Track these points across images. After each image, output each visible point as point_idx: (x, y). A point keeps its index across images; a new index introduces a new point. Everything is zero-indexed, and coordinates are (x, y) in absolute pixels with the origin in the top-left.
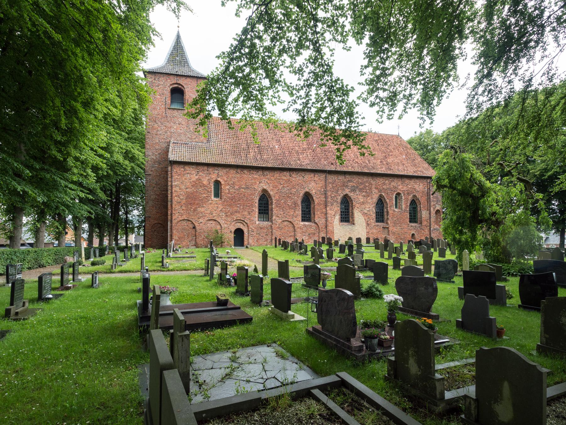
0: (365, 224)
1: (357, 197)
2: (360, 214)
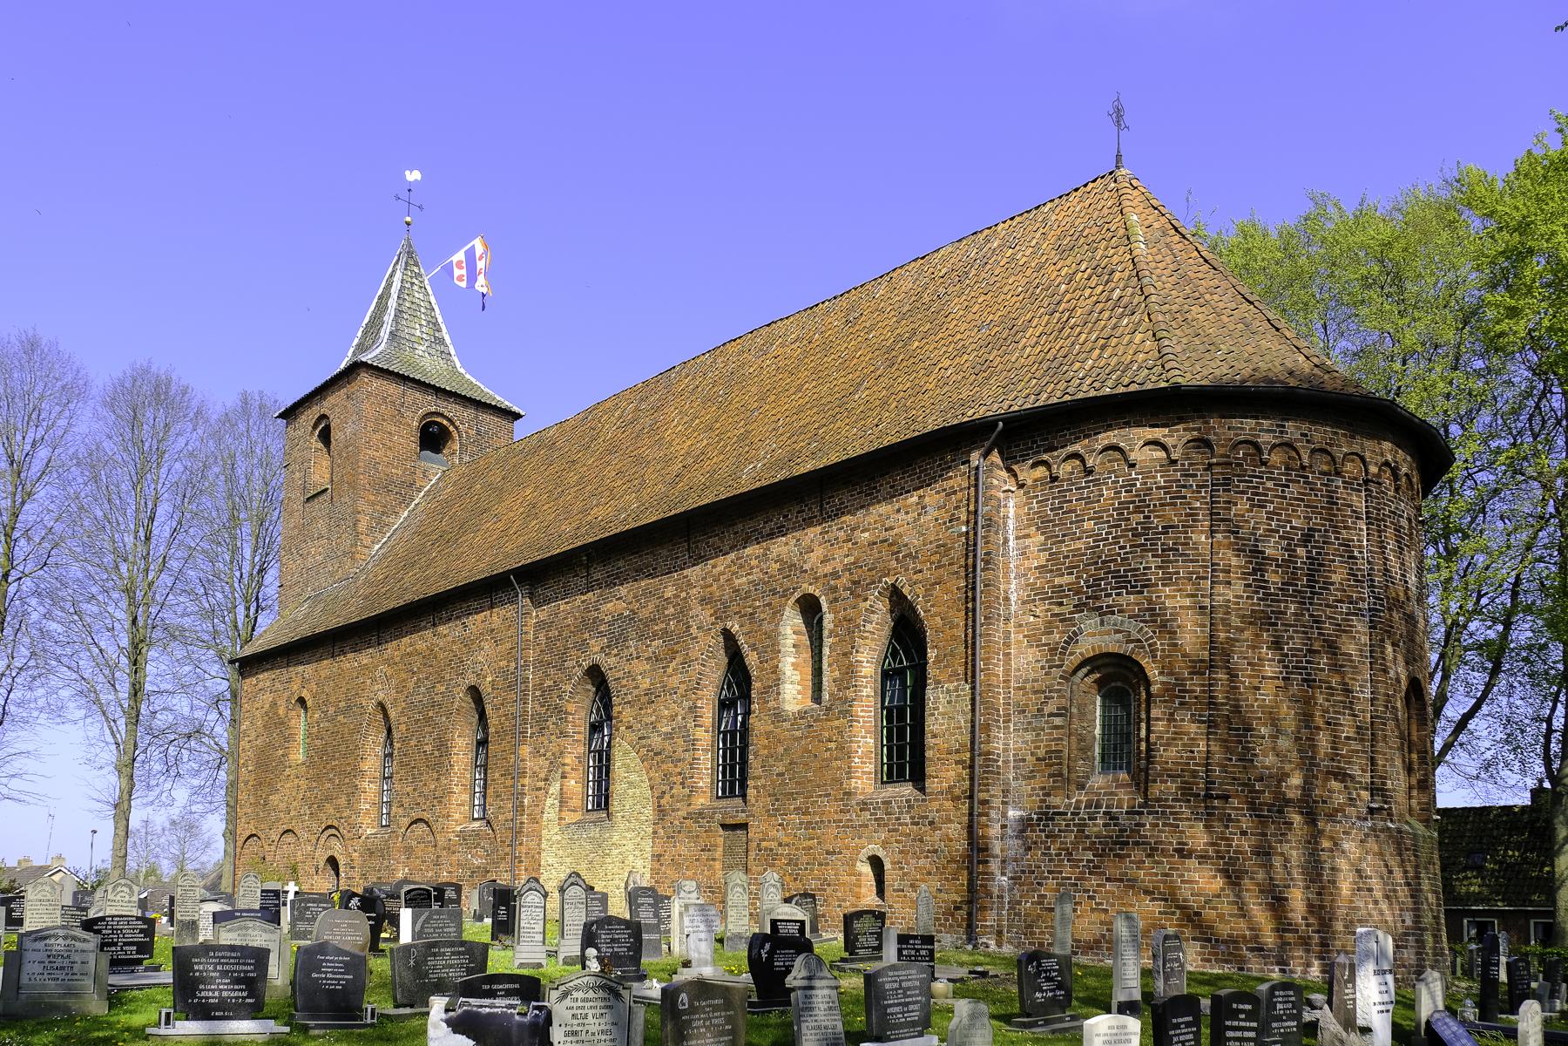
0: (649, 812)
1: (631, 672)
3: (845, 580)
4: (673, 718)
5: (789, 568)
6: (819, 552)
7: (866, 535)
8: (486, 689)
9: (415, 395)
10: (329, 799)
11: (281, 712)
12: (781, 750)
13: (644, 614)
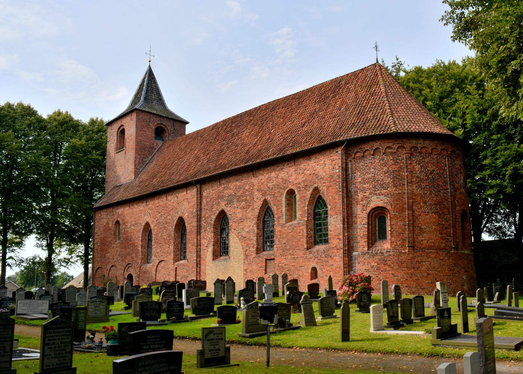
0: (242, 256)
1: (234, 213)
2: (236, 240)
3: (302, 184)
4: (249, 226)
5: (285, 181)
6: (294, 176)
7: (308, 172)
8: (185, 217)
9: (153, 118)
10: (129, 254)
11: (110, 226)
12: (284, 236)
13: (239, 194)
